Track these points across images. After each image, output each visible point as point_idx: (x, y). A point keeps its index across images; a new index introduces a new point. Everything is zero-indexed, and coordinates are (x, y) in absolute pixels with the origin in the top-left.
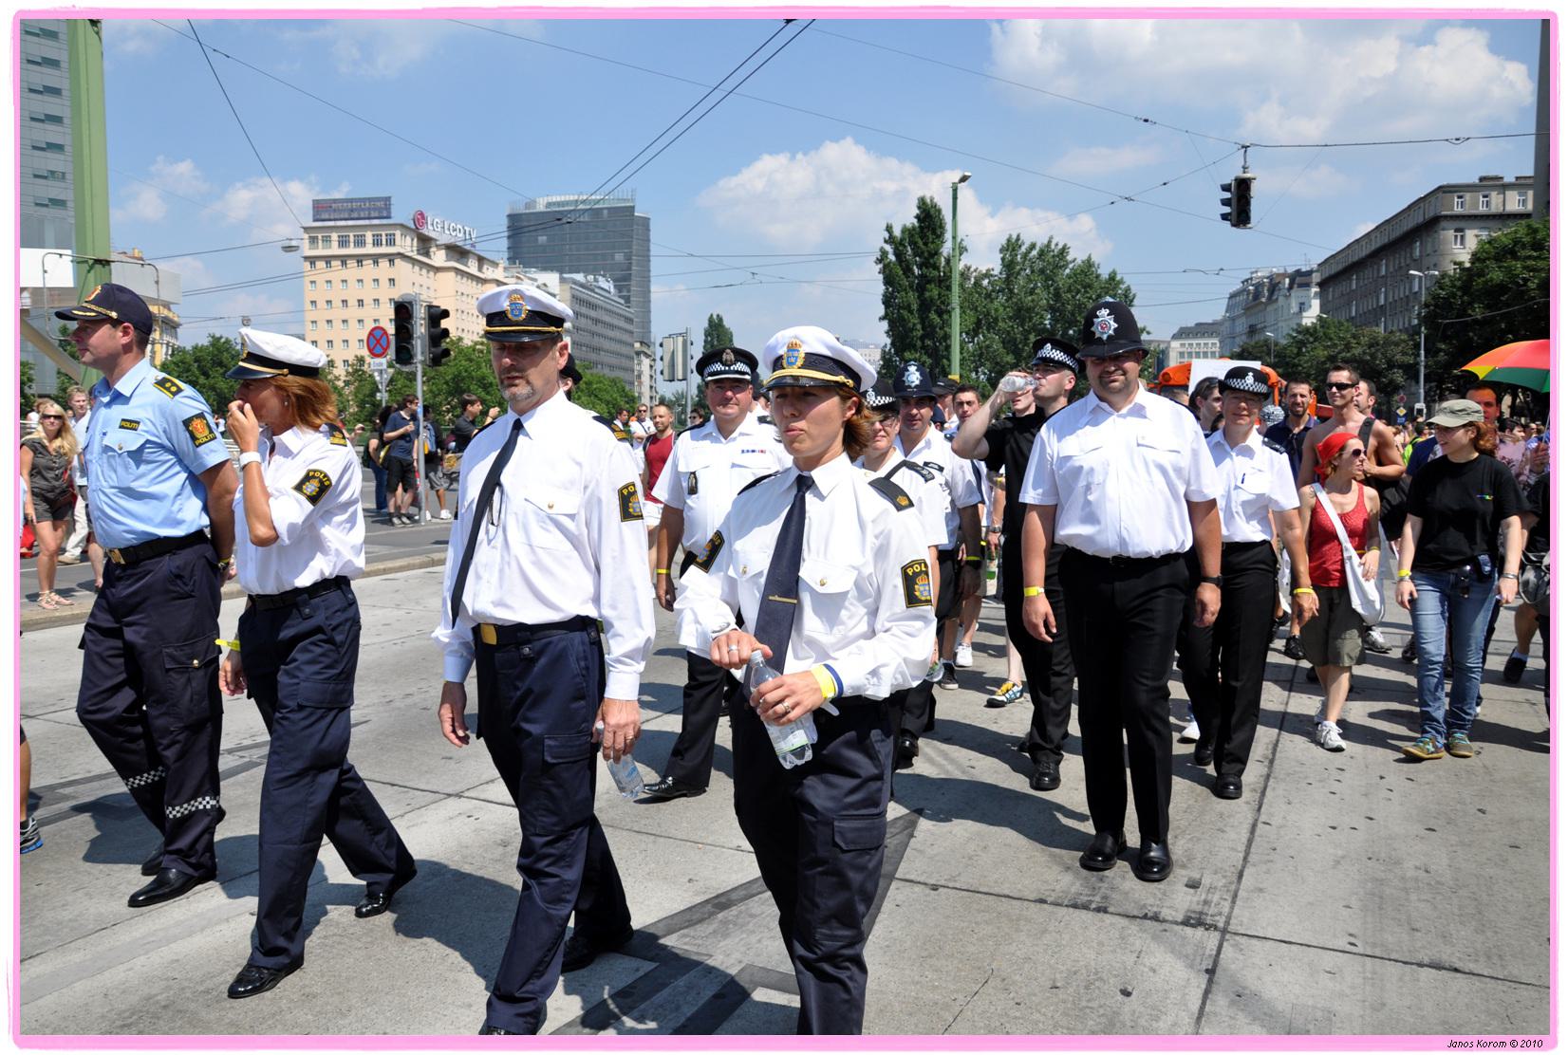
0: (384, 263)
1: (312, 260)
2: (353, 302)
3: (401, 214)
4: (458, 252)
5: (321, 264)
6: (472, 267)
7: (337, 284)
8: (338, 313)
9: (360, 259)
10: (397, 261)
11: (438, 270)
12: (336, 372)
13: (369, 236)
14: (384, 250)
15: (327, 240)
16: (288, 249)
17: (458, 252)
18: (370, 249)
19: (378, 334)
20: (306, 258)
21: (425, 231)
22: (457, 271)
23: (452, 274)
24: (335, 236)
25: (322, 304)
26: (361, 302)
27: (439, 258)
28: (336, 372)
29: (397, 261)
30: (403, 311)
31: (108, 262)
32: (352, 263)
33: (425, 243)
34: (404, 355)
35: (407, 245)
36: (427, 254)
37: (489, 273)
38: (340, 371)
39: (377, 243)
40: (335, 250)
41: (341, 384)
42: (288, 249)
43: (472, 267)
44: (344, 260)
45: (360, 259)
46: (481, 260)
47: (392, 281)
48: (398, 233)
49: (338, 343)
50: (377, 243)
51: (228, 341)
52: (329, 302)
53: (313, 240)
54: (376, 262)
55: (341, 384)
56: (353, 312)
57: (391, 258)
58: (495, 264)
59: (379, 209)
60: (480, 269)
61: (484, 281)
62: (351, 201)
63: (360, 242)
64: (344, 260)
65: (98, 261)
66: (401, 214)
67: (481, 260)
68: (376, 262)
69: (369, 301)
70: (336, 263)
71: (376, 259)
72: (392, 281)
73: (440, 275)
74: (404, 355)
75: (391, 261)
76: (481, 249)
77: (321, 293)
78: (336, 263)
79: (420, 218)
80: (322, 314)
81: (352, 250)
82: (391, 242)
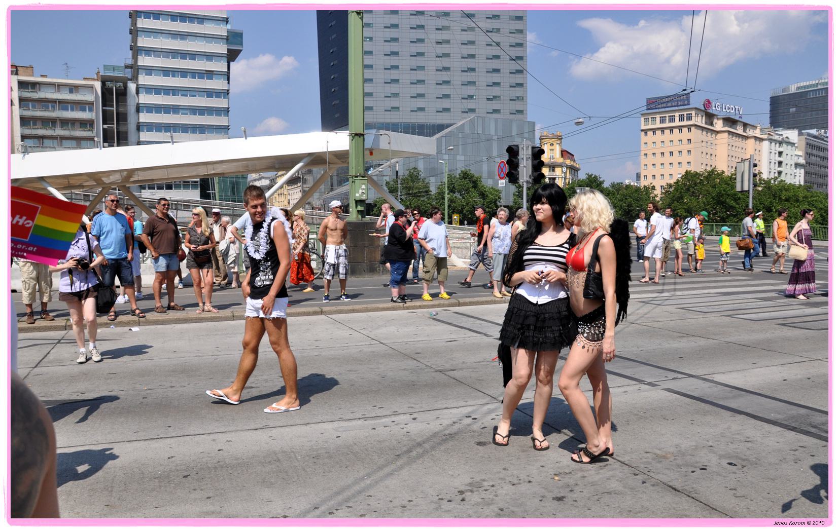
0: (685, 130)
1: (646, 131)
2: (667, 154)
3: (697, 101)
4: (730, 121)
5: (650, 133)
6: (740, 130)
7: (659, 144)
8: (659, 159)
9: (671, 129)
10: (693, 128)
11: (718, 132)
12: (655, 192)
13: (677, 119)
14: (685, 123)
15: (654, 119)
16: (578, 123)
17: (730, 121)
18: (677, 123)
19: (502, 165)
20: (642, 130)
21: (710, 111)
22: (729, 131)
23: (726, 135)
24: (658, 119)
25: (650, 156)
26: (671, 153)
27: (719, 125)
28: (655, 192)
29: (693, 128)
30: (513, 152)
31: (363, 135)
32: (667, 132)
33: (710, 117)
34: (513, 177)
35: (700, 120)
36: (712, 124)
37: (750, 132)
38: (658, 192)
39: (681, 118)
40: (658, 125)
41: (658, 199)
42: (578, 123)
43: (740, 130)
44: (663, 130)
45: (671, 129)
46: (745, 125)
47: (689, 140)
48: (693, 113)
49: (658, 177)
50: (681, 118)
51: (595, 177)
52: (654, 154)
53: (646, 120)
54: (681, 131)
55: (658, 199)
56: (667, 159)
57: (689, 128)
58: (754, 127)
59: (684, 101)
60: (744, 131)
61: (747, 138)
62: (668, 97)
63: (672, 119)
64: (663, 130)
65: (356, 135)
66: (697, 101)
67: (745, 125)
68: (681, 131)
69: (676, 154)
70: (659, 132)
71: (680, 128)
72: (689, 140)
73: (719, 135)
74: (513, 177)
75: (689, 130)
76: (744, 120)
77: (649, 149)
78: (659, 132)
79: (708, 103)
80: (650, 160)
81: (667, 124)
82: (689, 118)
